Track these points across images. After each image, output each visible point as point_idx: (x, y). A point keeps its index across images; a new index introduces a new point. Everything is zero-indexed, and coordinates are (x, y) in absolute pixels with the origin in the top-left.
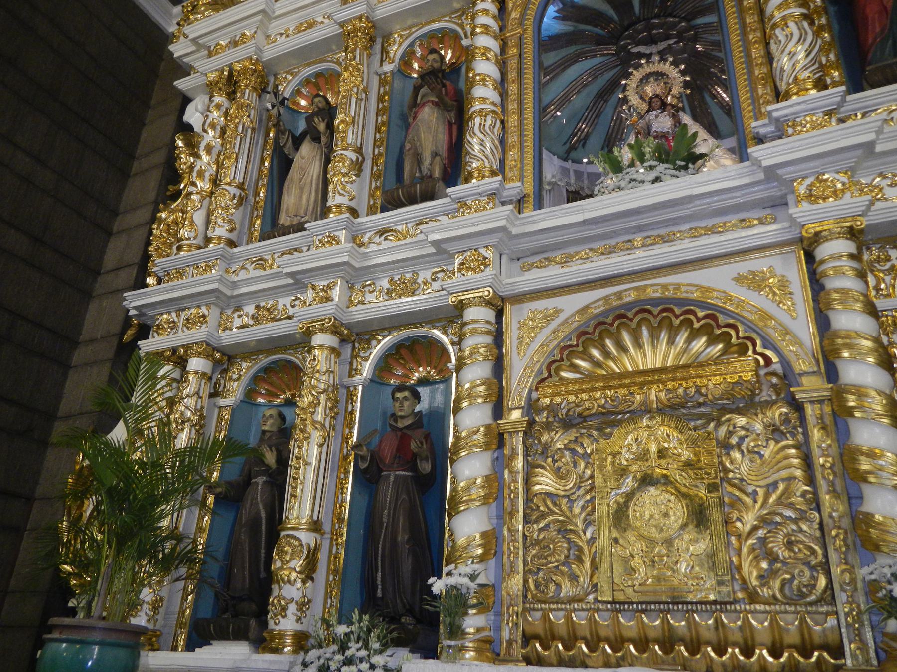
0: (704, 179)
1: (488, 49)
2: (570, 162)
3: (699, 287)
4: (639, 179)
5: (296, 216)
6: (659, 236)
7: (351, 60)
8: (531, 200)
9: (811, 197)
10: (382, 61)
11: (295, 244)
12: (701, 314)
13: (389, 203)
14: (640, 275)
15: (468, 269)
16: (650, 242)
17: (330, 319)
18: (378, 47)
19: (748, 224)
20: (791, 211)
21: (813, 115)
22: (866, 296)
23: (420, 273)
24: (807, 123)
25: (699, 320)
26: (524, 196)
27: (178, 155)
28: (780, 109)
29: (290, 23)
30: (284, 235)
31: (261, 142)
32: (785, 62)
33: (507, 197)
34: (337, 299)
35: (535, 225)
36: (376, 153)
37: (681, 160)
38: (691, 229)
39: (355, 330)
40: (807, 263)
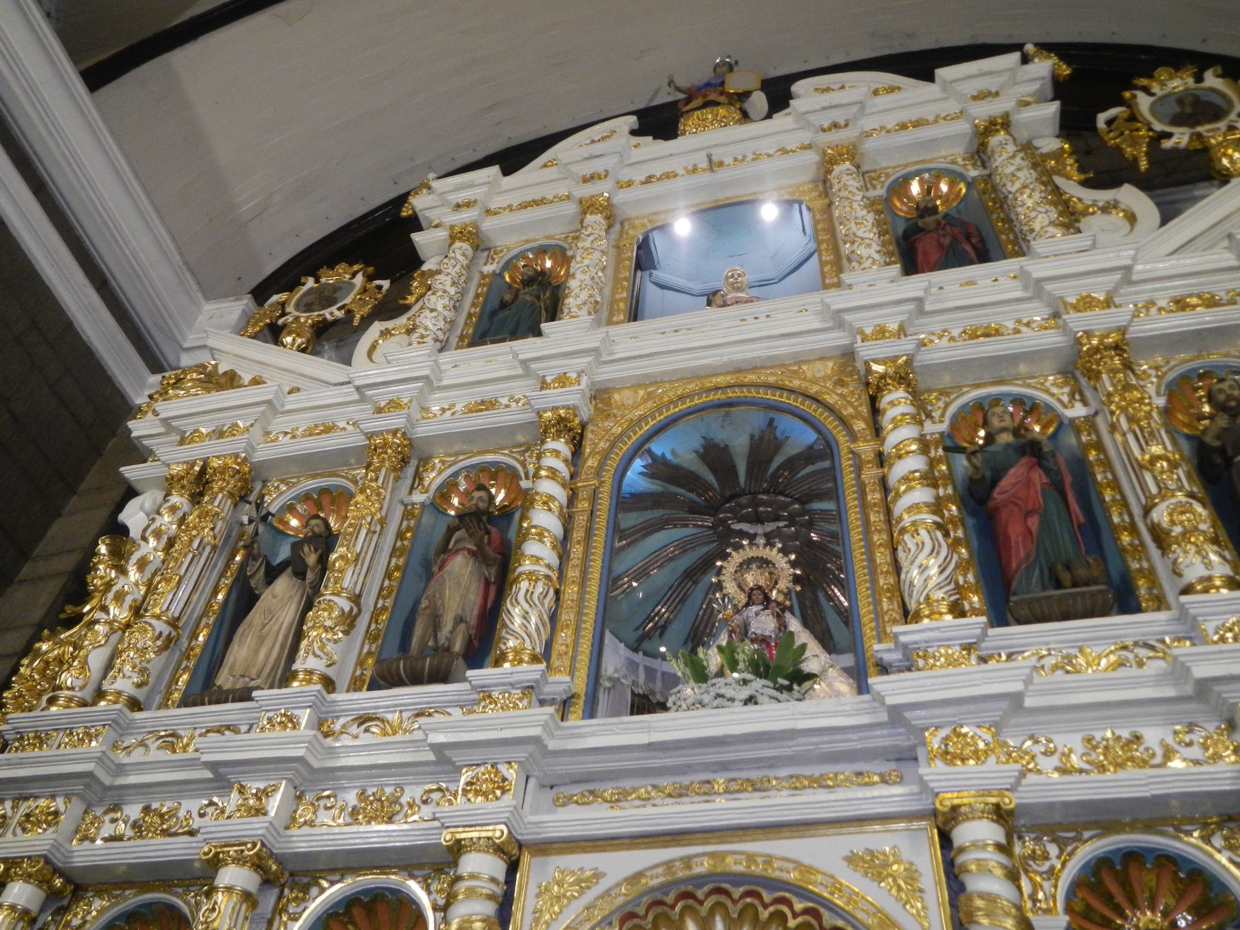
0: (811, 710)
1: (551, 498)
2: (641, 653)
3: (798, 865)
4: (728, 695)
5: (243, 676)
6: (748, 780)
7: (371, 480)
8: (581, 702)
9: (946, 756)
10: (412, 488)
11: (231, 719)
12: (799, 906)
13: (383, 678)
14: (718, 834)
15: (477, 793)
16: (736, 787)
17: (254, 845)
18: (410, 470)
19: (867, 779)
20: (923, 770)
21: (949, 646)
22: (1019, 908)
23: (407, 789)
24: (941, 655)
25: (795, 915)
26: (572, 697)
27: (96, 564)
28: (909, 633)
29: (302, 422)
30: (218, 702)
31: (220, 565)
32: (913, 575)
33: (548, 694)
34: (272, 814)
35: (581, 740)
36: (379, 605)
37: (786, 677)
38: (791, 777)
39: (291, 867)
40: (942, 847)
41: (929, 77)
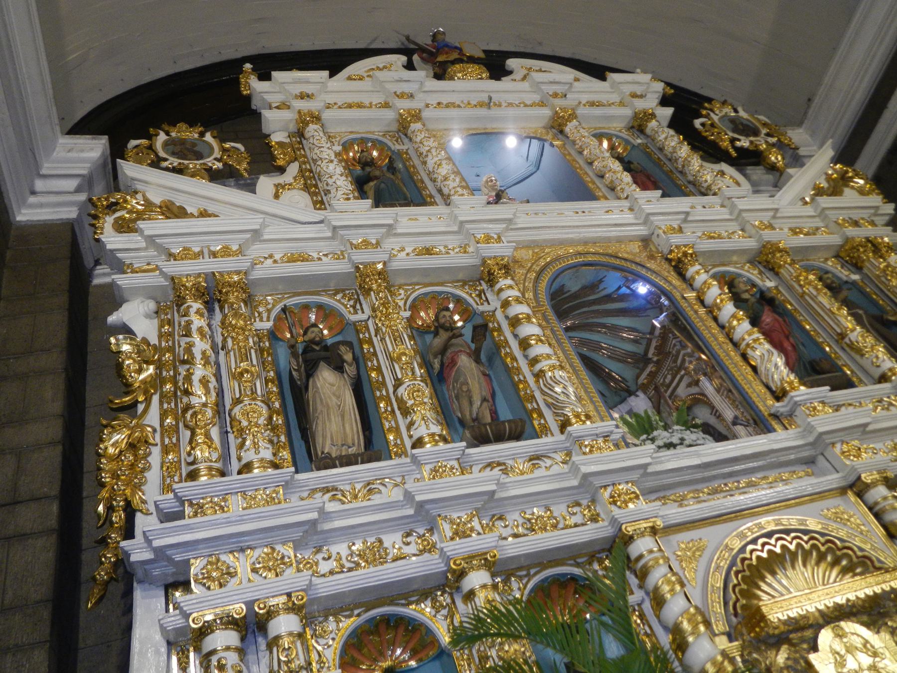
5: (343, 445)
12: (822, 540)
30: (326, 468)
35: (663, 465)
41: (604, 79)
